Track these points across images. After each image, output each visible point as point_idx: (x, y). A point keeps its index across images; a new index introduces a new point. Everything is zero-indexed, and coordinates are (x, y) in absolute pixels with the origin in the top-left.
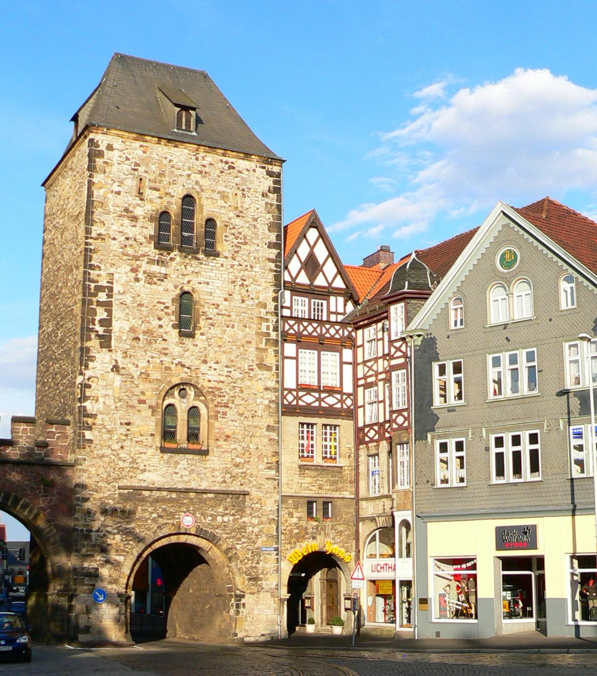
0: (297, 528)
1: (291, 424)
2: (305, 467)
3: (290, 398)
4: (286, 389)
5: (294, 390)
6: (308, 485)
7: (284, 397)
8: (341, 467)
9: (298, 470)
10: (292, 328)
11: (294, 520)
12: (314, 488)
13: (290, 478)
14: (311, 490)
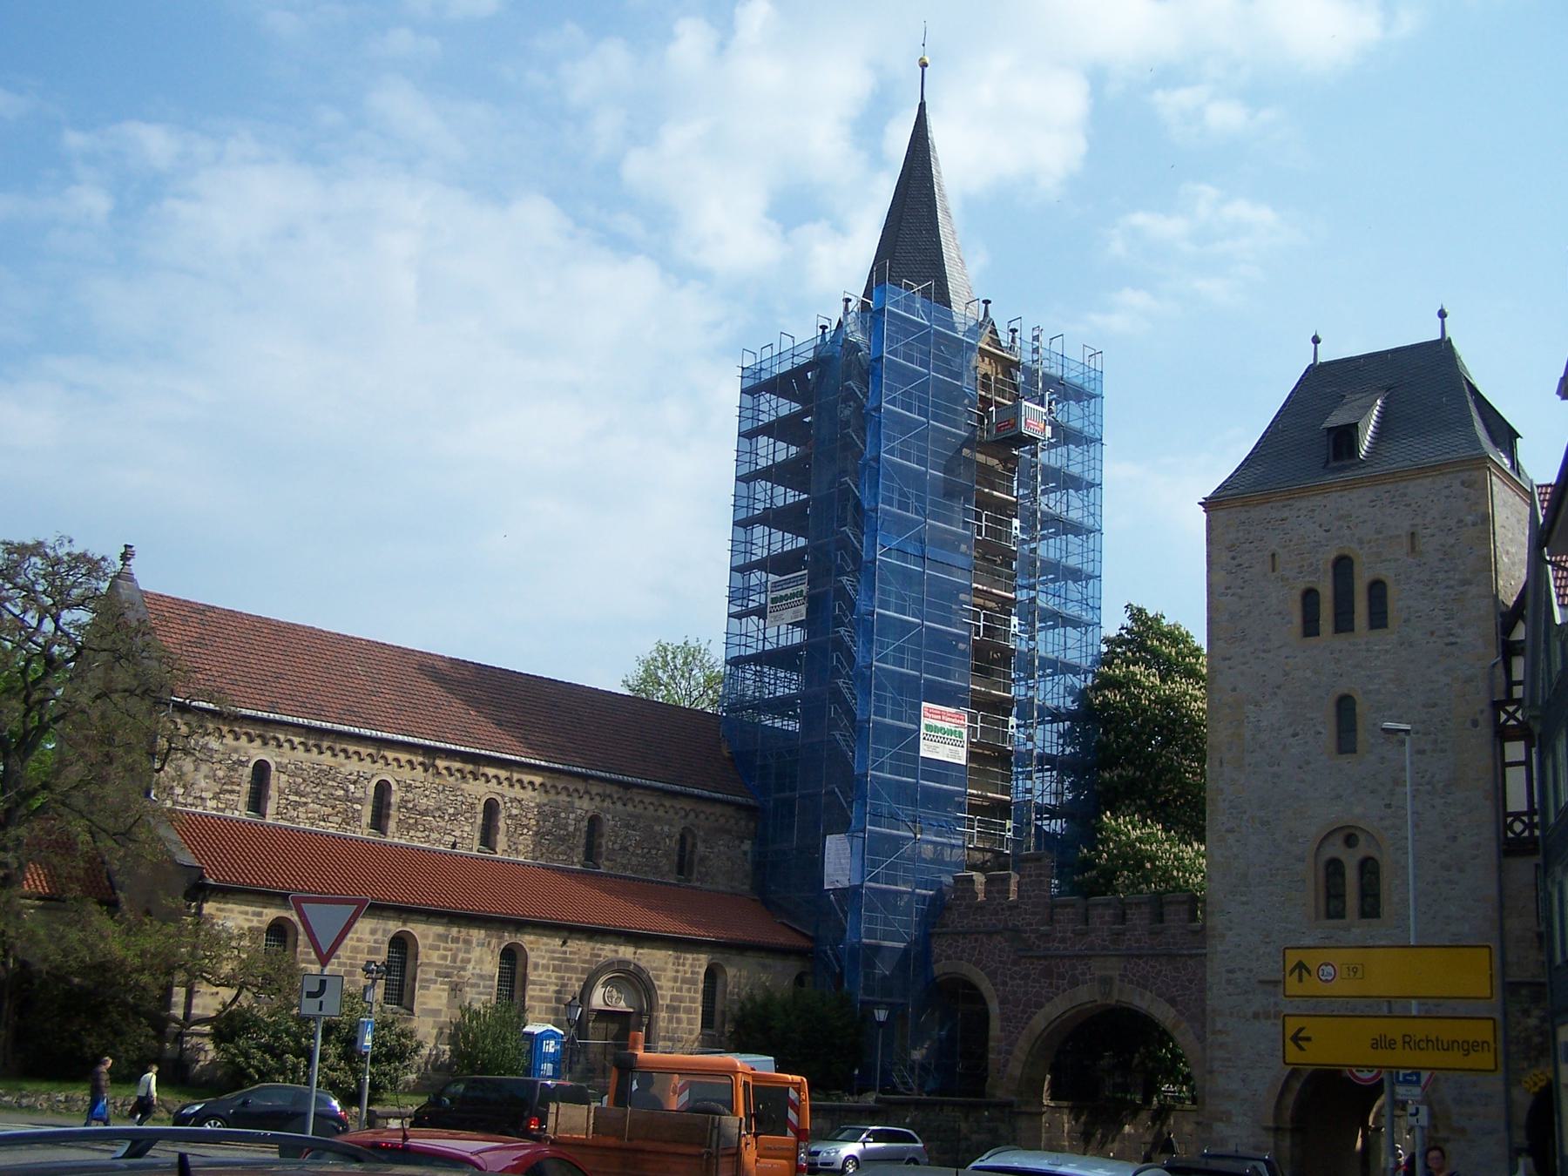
1: (1523, 869)
3: (1518, 827)
4: (1511, 814)
5: (1524, 814)
7: (1510, 827)
11: (1532, 1022)
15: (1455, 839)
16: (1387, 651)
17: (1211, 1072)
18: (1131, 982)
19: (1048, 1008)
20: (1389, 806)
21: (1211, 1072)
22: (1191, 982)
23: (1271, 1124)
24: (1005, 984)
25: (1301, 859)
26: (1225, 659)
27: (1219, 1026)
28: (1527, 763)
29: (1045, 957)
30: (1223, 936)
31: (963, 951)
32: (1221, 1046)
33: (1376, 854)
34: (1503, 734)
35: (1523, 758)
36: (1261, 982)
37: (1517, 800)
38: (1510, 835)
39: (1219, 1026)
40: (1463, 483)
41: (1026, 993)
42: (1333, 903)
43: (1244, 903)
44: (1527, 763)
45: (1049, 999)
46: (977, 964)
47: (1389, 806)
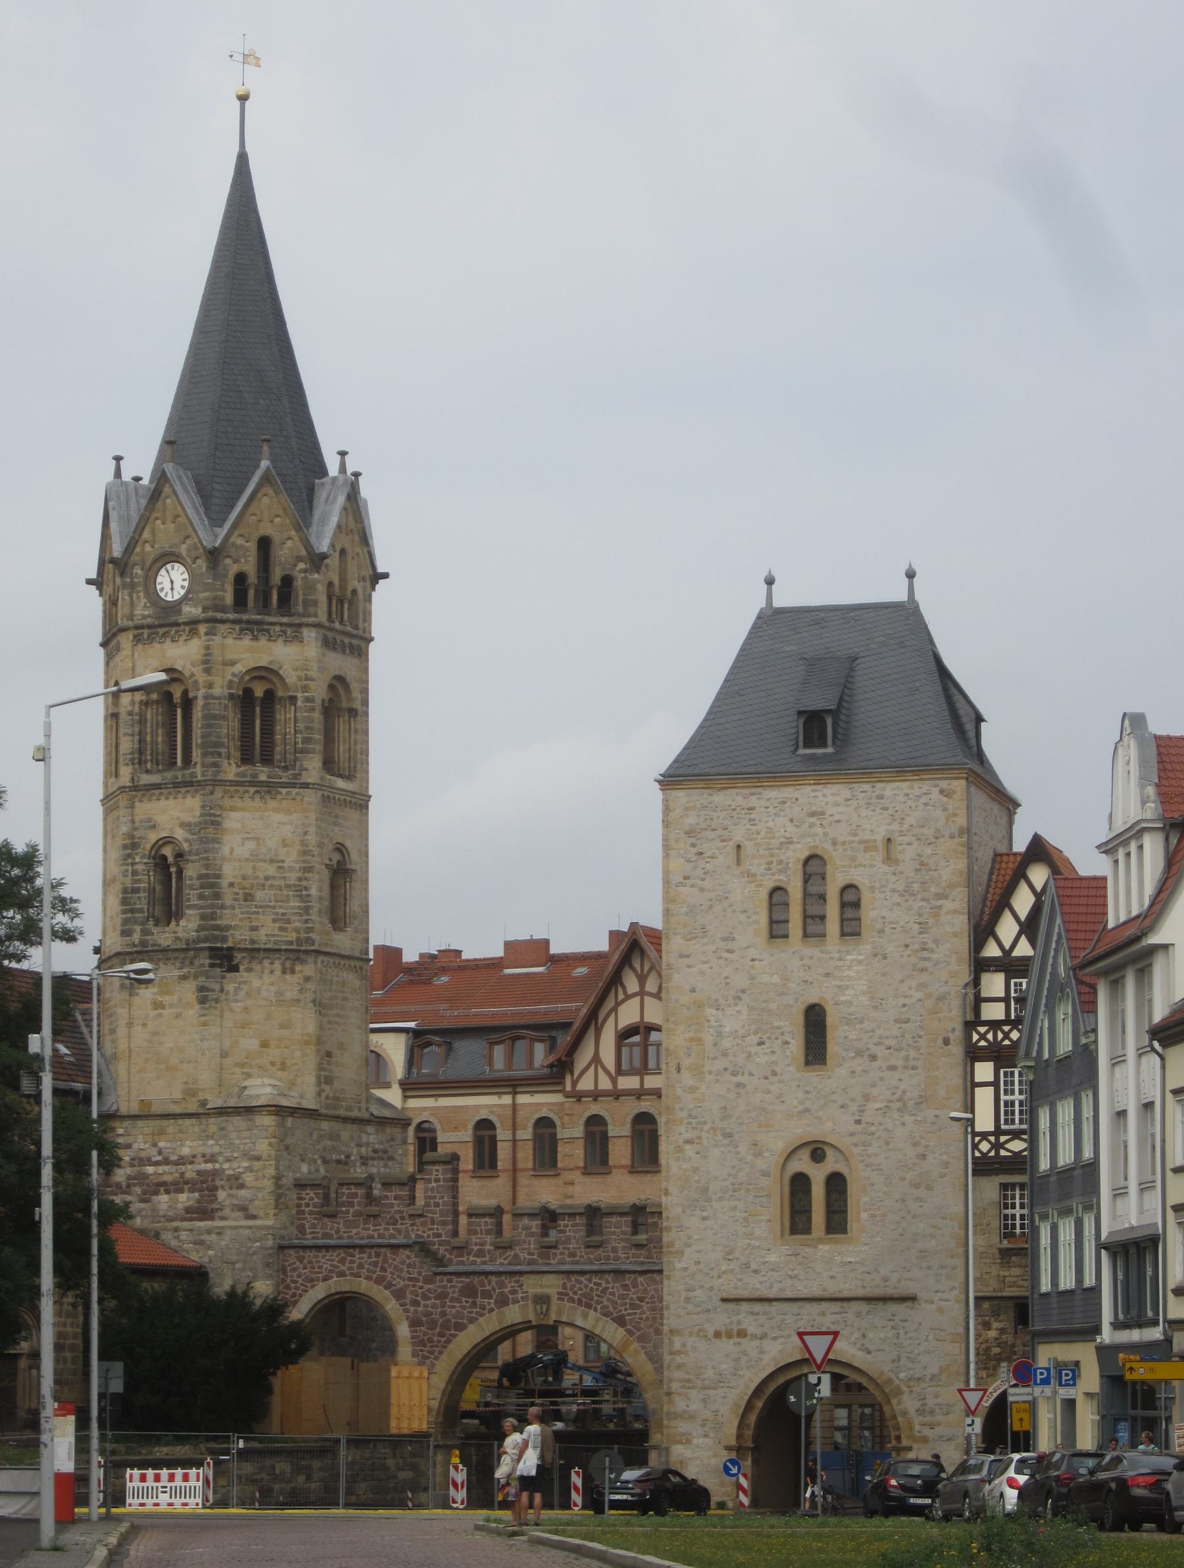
0: (999, 1345)
1: (990, 1187)
3: (985, 1146)
5: (990, 1133)
7: (975, 1146)
9: (998, 1256)
10: (982, 1037)
11: (992, 1334)
13: (985, 1270)
15: (924, 1157)
16: (860, 962)
17: (669, 1394)
18: (572, 1300)
20: (858, 1122)
21: (669, 1394)
22: (641, 1299)
23: (733, 1443)
24: (415, 1303)
25: (765, 1174)
26: (682, 956)
27: (677, 1346)
28: (995, 1084)
29: (467, 1274)
30: (682, 1253)
31: (361, 1266)
32: (679, 1367)
33: (844, 1170)
34: (974, 1055)
35: (992, 1079)
36: (724, 1300)
37: (984, 1121)
38: (977, 1154)
39: (677, 1346)
40: (941, 792)
41: (443, 1314)
42: (798, 1220)
43: (704, 1219)
44: (995, 1084)
45: (472, 1320)
46: (379, 1281)
47: (858, 1122)
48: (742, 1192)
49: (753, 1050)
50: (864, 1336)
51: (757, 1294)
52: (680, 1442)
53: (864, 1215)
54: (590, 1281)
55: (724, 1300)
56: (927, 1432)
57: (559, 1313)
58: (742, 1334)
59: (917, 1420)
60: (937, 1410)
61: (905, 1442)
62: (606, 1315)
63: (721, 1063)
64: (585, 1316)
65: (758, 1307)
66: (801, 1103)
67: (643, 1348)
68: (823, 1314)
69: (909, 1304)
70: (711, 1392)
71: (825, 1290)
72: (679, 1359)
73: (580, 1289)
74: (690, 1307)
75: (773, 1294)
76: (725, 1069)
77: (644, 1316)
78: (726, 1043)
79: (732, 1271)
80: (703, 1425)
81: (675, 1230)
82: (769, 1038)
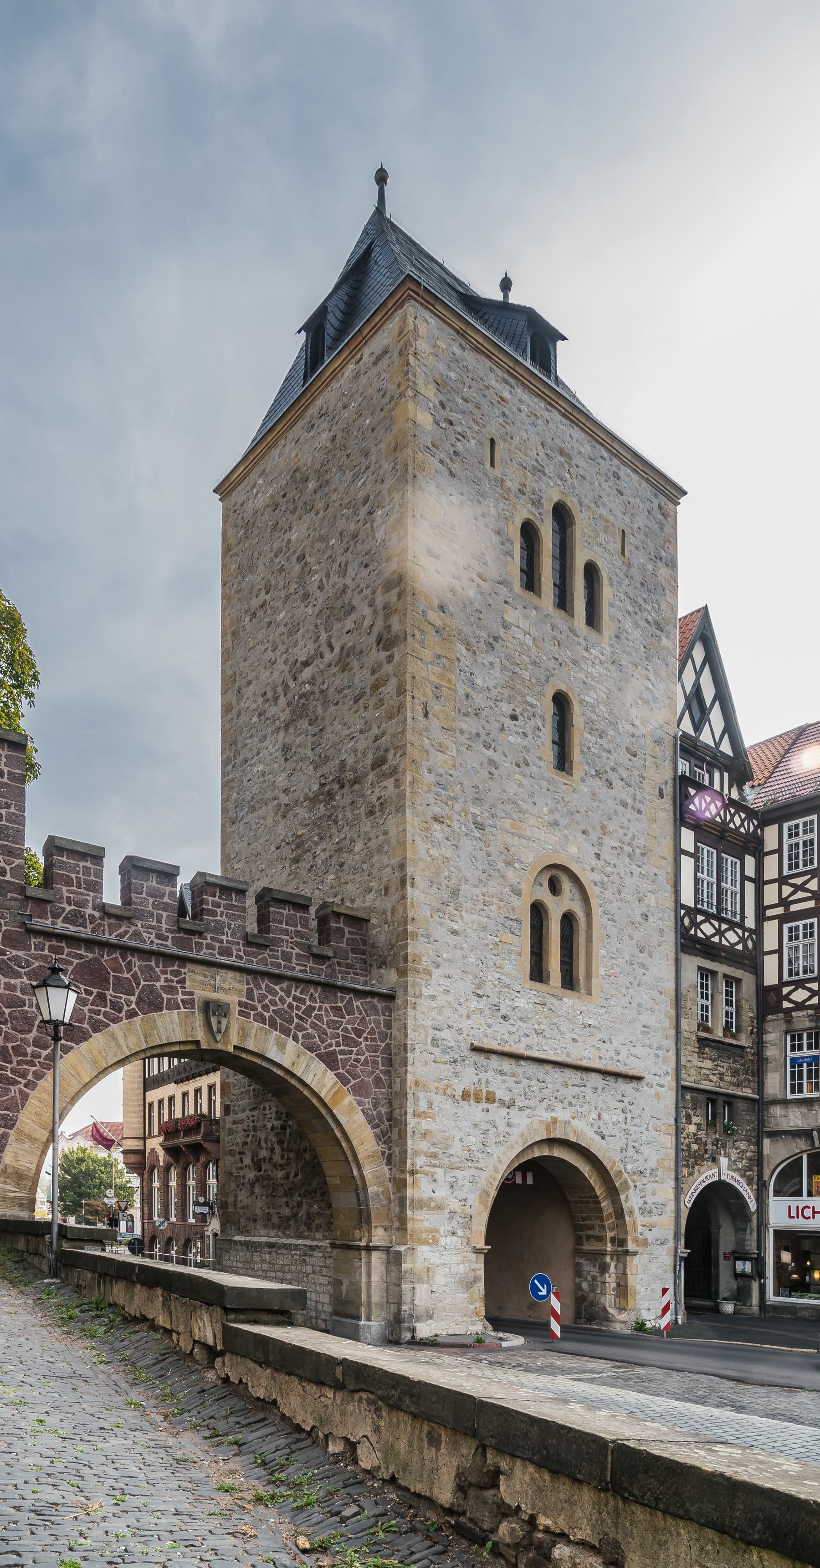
1: (691, 964)
2: (705, 1042)
6: (708, 1072)
8: (743, 1048)
12: (714, 1078)
14: (711, 1081)
16: (602, 663)
18: (262, 1020)
19: (97, 1040)
22: (359, 1033)
27: (423, 1106)
32: (424, 1136)
39: (423, 1106)
43: (454, 932)
48: (493, 908)
49: (508, 722)
50: (599, 1117)
51: (507, 1049)
52: (427, 1243)
53: (602, 971)
54: (288, 994)
55: (475, 1049)
56: (648, 1235)
57: (244, 1033)
58: (490, 1098)
59: (640, 1220)
60: (654, 1210)
61: (631, 1246)
62: (311, 1048)
63: (470, 725)
64: (282, 1046)
65: (507, 1065)
66: (551, 812)
67: (360, 1103)
68: (566, 1085)
69: (634, 1084)
70: (458, 1173)
71: (568, 1055)
72: (425, 1124)
73: (275, 1004)
74: (437, 1051)
75: (521, 1049)
76: (478, 735)
77: (362, 1058)
78: (479, 700)
79: (481, 1012)
80: (450, 1219)
81: (421, 939)
82: (521, 714)
